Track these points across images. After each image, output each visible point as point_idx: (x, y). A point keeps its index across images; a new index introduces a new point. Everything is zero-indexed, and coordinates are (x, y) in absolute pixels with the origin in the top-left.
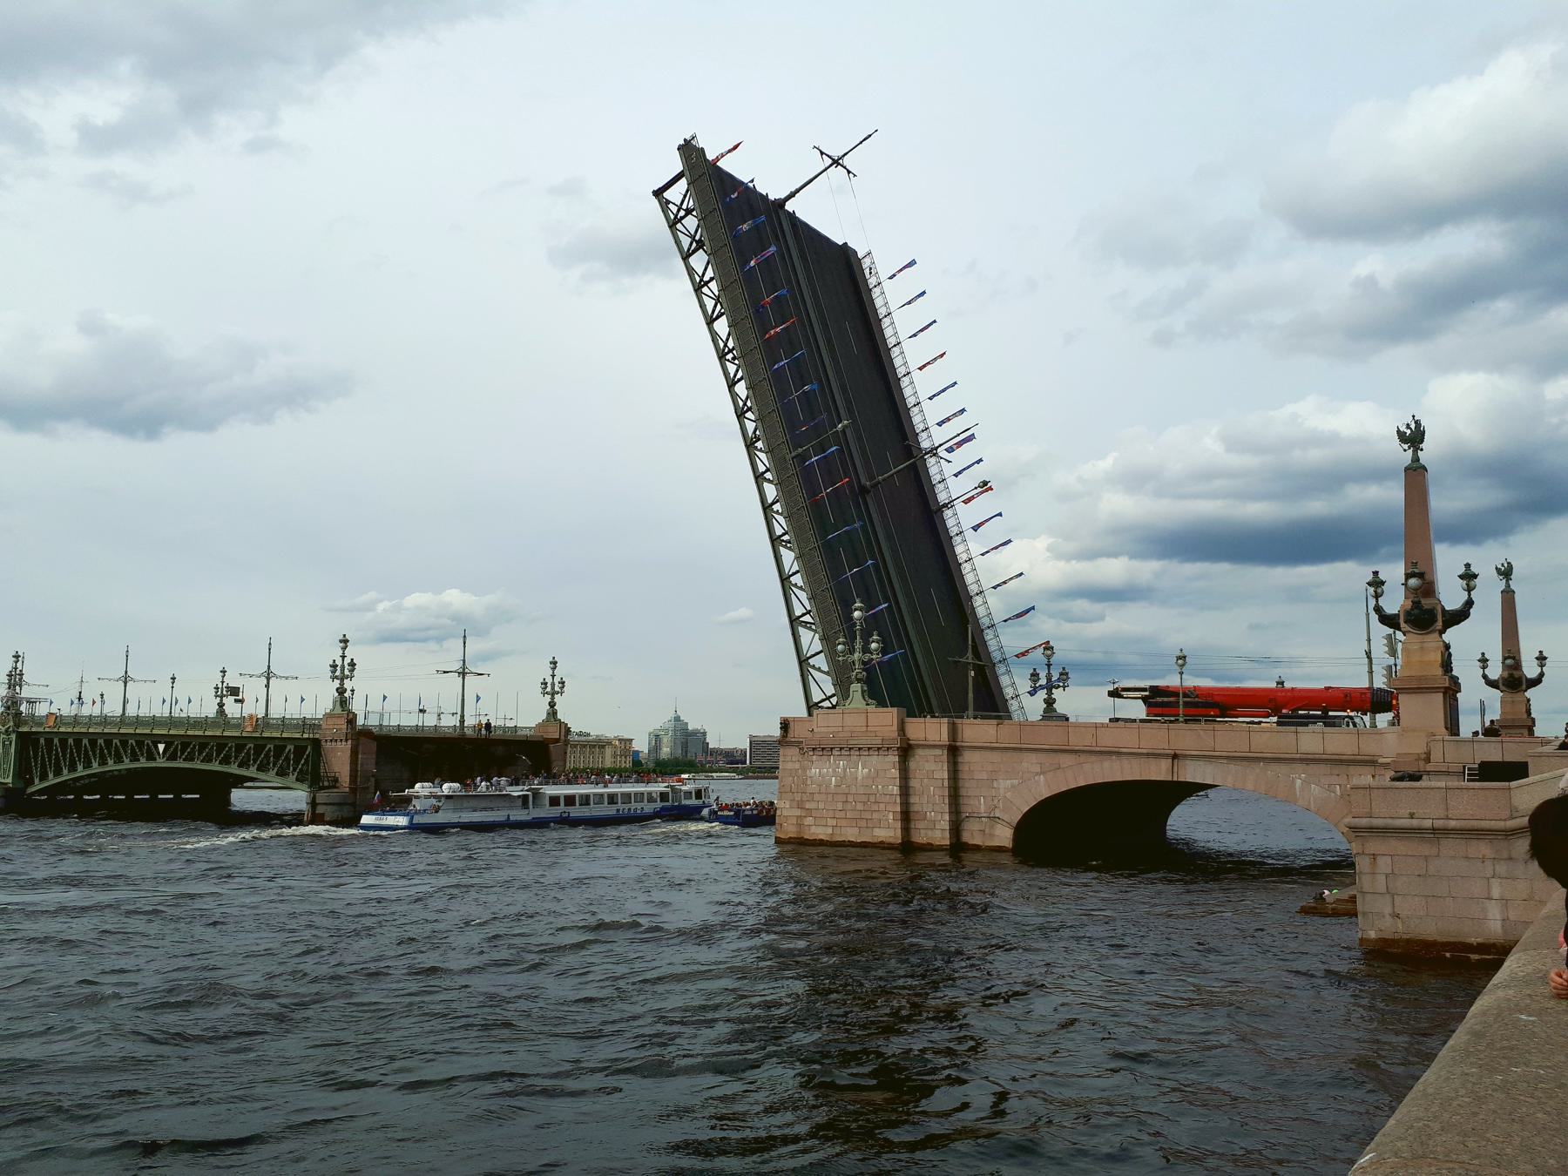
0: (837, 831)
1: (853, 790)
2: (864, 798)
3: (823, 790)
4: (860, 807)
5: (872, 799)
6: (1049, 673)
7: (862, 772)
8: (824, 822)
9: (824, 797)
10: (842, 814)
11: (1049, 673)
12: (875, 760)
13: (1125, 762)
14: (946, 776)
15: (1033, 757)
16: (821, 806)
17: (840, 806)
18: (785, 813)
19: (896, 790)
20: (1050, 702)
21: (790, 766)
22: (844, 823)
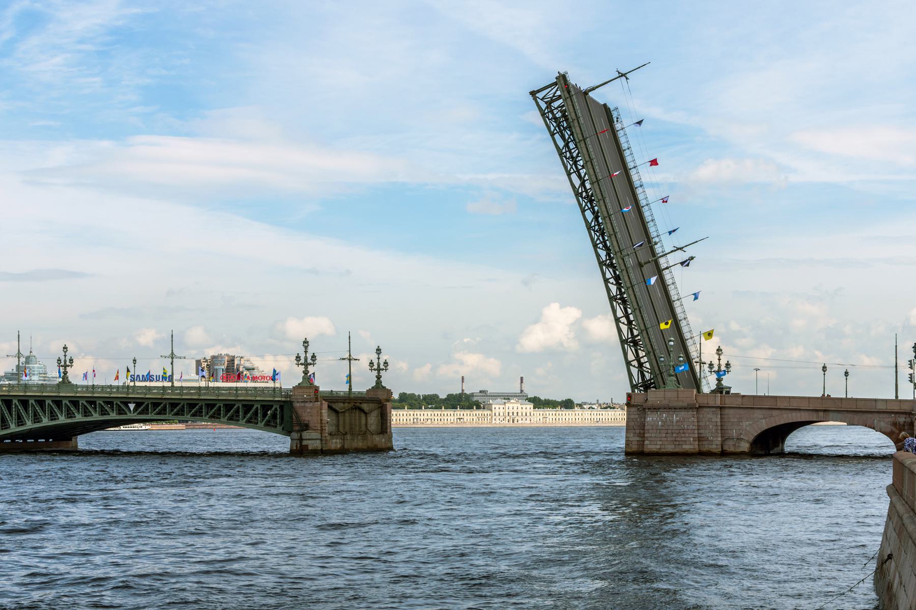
0: (663, 447)
1: (671, 428)
2: (677, 431)
3: (654, 427)
4: (674, 435)
5: (681, 431)
6: (719, 364)
8: (655, 443)
10: (665, 439)
11: (719, 364)
13: (802, 413)
14: (719, 420)
15: (759, 411)
17: (664, 435)
20: (719, 380)
22: (666, 443)
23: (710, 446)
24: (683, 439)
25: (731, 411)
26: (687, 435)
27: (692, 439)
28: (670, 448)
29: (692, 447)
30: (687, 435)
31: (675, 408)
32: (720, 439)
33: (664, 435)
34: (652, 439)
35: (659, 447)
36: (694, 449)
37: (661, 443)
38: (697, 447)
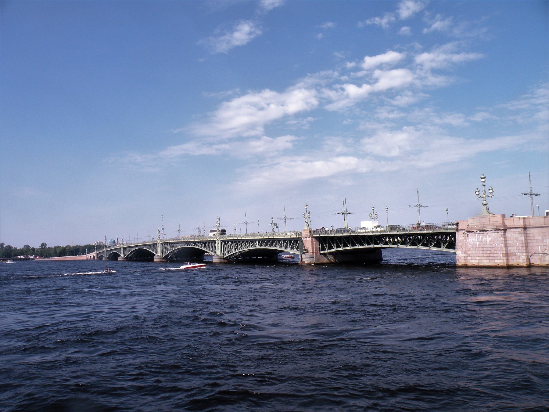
0: (480, 261)
1: (486, 246)
2: (490, 249)
3: (474, 247)
4: (489, 252)
5: (494, 249)
7: (488, 239)
8: (475, 258)
9: (475, 249)
12: (494, 235)
16: (474, 252)
17: (481, 252)
18: (460, 256)
19: (503, 245)
21: (460, 238)
22: (483, 258)
23: (518, 260)
24: (495, 255)
25: (536, 230)
26: (498, 252)
27: (501, 255)
28: (486, 262)
29: (502, 262)
30: (498, 252)
31: (488, 231)
32: (525, 254)
33: (481, 252)
34: (472, 255)
35: (477, 261)
36: (504, 263)
37: (479, 258)
38: (505, 261)
